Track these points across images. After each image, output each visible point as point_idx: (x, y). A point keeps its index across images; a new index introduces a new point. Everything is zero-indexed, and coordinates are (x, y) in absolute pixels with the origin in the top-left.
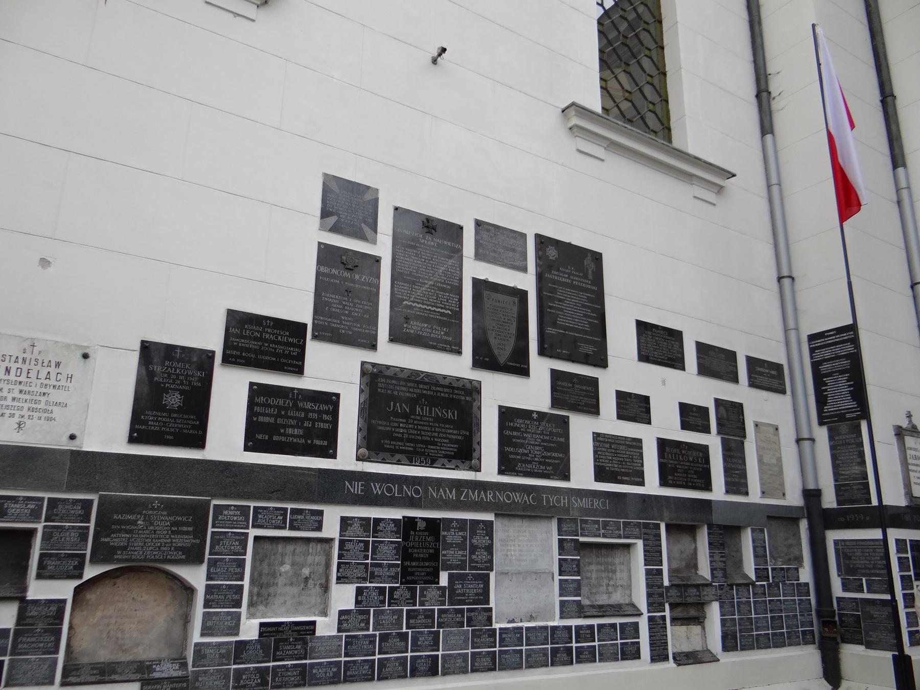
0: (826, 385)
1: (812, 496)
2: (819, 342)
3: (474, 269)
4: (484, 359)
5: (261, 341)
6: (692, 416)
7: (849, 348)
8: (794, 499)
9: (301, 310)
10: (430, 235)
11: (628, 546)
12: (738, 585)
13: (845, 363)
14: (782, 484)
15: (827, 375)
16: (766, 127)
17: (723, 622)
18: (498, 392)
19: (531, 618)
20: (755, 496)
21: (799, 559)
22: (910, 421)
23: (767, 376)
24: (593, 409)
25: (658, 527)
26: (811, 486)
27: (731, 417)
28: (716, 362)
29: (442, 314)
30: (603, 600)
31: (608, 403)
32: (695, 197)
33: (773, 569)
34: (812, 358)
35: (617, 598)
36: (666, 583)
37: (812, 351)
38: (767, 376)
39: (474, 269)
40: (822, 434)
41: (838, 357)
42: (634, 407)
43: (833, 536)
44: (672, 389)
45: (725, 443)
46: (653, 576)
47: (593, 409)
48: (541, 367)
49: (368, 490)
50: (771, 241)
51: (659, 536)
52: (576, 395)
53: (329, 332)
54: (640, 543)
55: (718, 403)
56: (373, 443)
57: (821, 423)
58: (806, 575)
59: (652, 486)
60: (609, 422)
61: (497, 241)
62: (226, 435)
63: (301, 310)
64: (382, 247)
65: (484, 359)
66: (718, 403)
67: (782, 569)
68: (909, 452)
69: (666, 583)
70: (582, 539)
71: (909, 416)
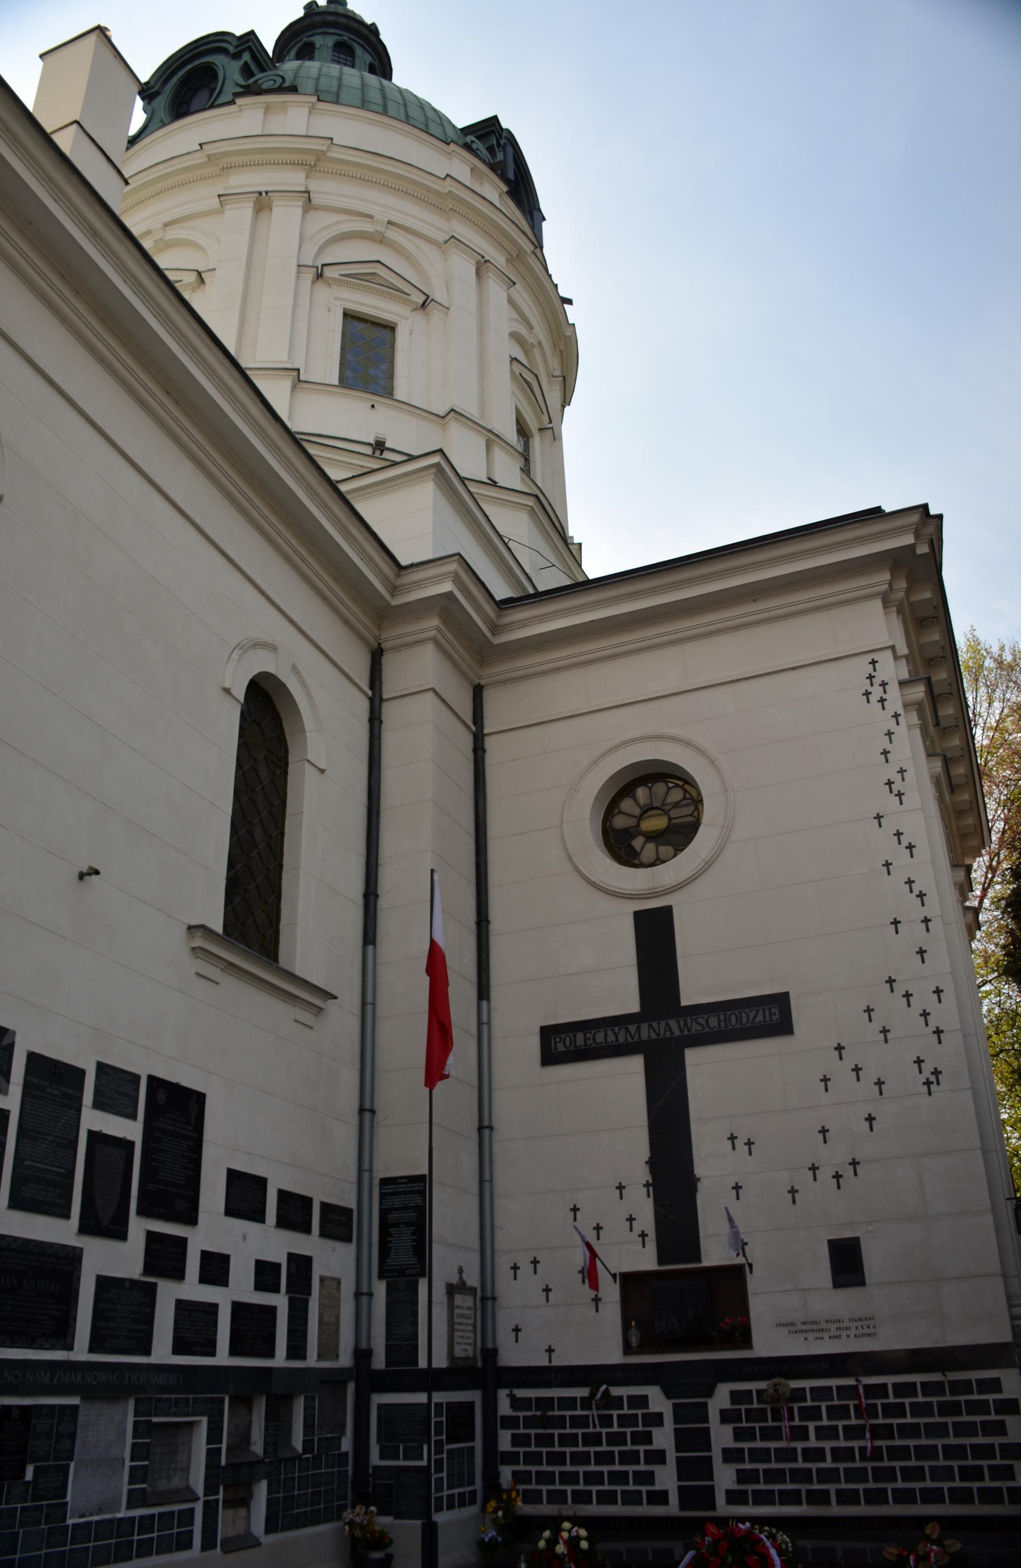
0: (391, 1236)
1: (362, 1355)
2: (390, 1189)
4: (91, 1225)
6: (266, 1275)
7: (418, 1200)
8: (345, 1360)
11: (191, 1424)
12: (286, 1460)
13: (412, 1215)
14: (337, 1345)
15: (396, 1225)
16: (369, 936)
17: (269, 1501)
19: (100, 1511)
20: (312, 1361)
21: (343, 1426)
22: (461, 1277)
23: (338, 1223)
24: (179, 1274)
25: (222, 1400)
26: (364, 1346)
28: (295, 1212)
29: (58, 1174)
30: (163, 1485)
32: (296, 1021)
33: (319, 1440)
34: (381, 1204)
35: (176, 1482)
36: (223, 1462)
37: (382, 1196)
38: (338, 1223)
39: (93, 1119)
40: (380, 1289)
41: (406, 1208)
42: (216, 1270)
43: (379, 1399)
45: (292, 1303)
46: (213, 1455)
47: (179, 1274)
48: (138, 1227)
50: (358, 1066)
51: (222, 1410)
54: (205, 1420)
55: (291, 1257)
57: (381, 1277)
58: (346, 1444)
61: (116, 1087)
66: (291, 1257)
67: (327, 1439)
68: (457, 1311)
69: (223, 1462)
70: (155, 1420)
71: (461, 1271)
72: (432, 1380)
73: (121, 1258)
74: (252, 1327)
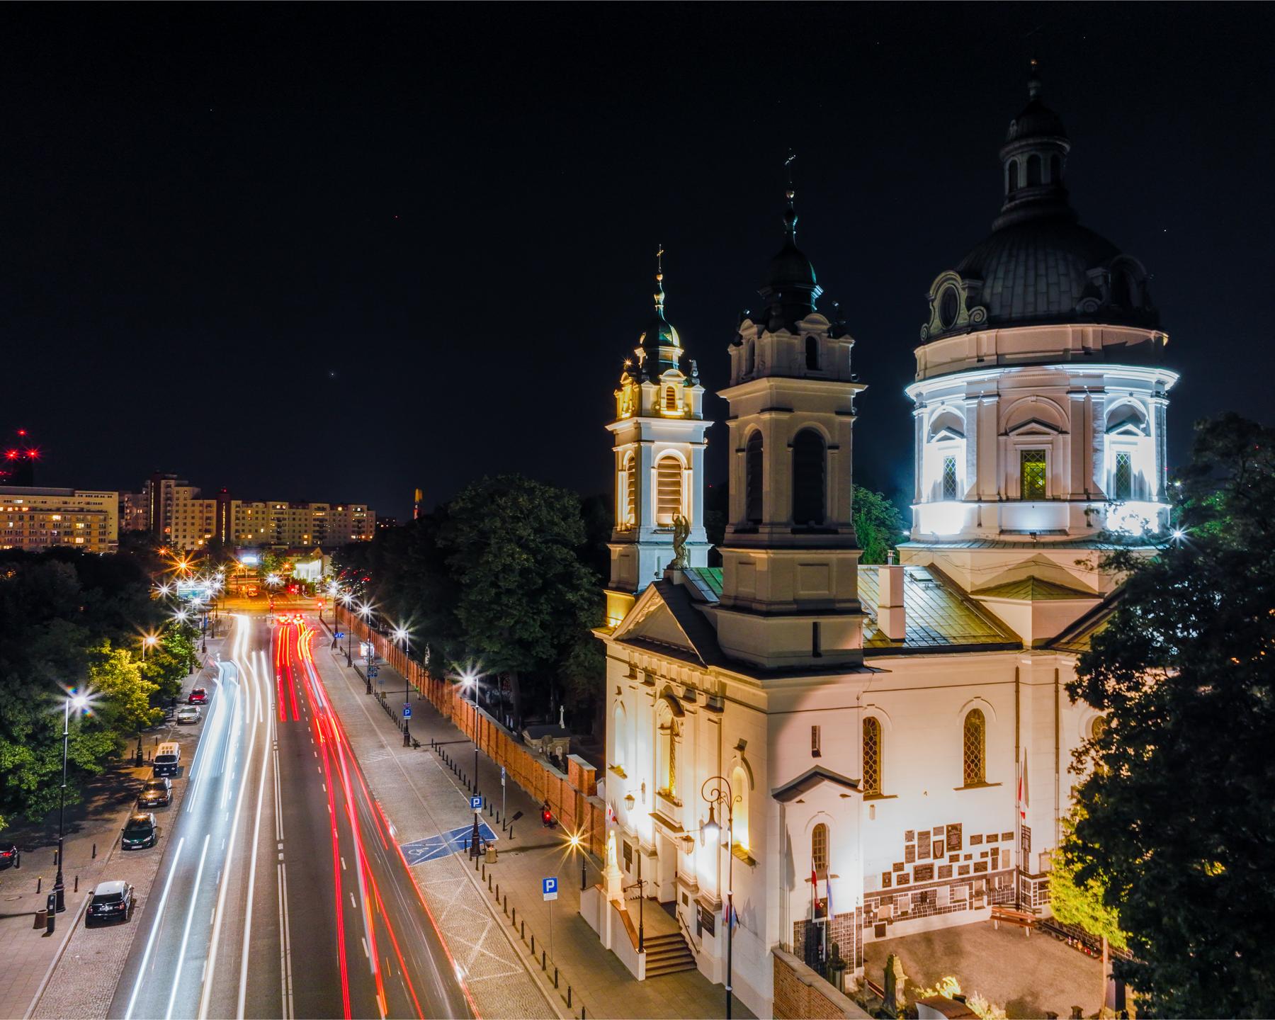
3: (933, 838)
4: (935, 857)
5: (898, 867)
6: (984, 855)
9: (903, 860)
10: (924, 835)
18: (938, 863)
20: (1000, 869)
27: (995, 852)
31: (962, 858)
42: (968, 857)
44: (976, 851)
48: (947, 855)
49: (915, 888)
52: (954, 859)
53: (908, 862)
56: (916, 879)
59: (972, 874)
60: (962, 862)
61: (938, 831)
62: (894, 885)
63: (903, 860)
64: (915, 842)
65: (935, 857)
72: (1033, 877)
73: (945, 861)
74: (980, 867)
